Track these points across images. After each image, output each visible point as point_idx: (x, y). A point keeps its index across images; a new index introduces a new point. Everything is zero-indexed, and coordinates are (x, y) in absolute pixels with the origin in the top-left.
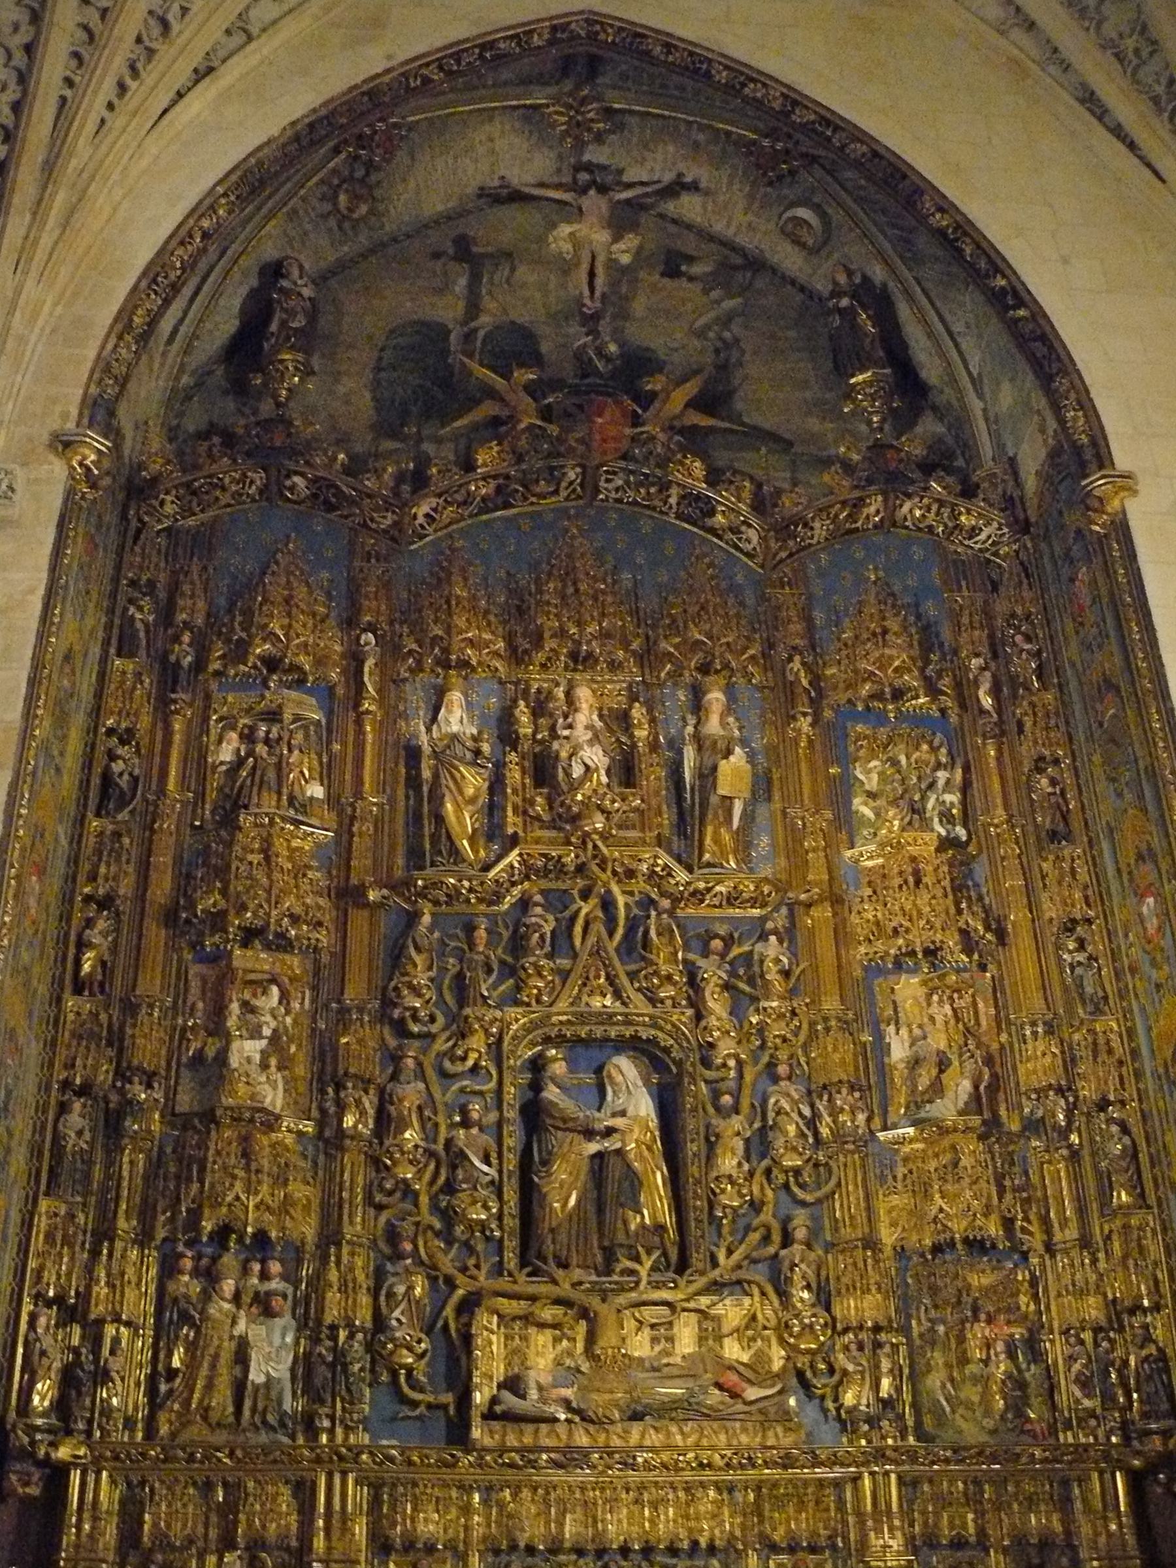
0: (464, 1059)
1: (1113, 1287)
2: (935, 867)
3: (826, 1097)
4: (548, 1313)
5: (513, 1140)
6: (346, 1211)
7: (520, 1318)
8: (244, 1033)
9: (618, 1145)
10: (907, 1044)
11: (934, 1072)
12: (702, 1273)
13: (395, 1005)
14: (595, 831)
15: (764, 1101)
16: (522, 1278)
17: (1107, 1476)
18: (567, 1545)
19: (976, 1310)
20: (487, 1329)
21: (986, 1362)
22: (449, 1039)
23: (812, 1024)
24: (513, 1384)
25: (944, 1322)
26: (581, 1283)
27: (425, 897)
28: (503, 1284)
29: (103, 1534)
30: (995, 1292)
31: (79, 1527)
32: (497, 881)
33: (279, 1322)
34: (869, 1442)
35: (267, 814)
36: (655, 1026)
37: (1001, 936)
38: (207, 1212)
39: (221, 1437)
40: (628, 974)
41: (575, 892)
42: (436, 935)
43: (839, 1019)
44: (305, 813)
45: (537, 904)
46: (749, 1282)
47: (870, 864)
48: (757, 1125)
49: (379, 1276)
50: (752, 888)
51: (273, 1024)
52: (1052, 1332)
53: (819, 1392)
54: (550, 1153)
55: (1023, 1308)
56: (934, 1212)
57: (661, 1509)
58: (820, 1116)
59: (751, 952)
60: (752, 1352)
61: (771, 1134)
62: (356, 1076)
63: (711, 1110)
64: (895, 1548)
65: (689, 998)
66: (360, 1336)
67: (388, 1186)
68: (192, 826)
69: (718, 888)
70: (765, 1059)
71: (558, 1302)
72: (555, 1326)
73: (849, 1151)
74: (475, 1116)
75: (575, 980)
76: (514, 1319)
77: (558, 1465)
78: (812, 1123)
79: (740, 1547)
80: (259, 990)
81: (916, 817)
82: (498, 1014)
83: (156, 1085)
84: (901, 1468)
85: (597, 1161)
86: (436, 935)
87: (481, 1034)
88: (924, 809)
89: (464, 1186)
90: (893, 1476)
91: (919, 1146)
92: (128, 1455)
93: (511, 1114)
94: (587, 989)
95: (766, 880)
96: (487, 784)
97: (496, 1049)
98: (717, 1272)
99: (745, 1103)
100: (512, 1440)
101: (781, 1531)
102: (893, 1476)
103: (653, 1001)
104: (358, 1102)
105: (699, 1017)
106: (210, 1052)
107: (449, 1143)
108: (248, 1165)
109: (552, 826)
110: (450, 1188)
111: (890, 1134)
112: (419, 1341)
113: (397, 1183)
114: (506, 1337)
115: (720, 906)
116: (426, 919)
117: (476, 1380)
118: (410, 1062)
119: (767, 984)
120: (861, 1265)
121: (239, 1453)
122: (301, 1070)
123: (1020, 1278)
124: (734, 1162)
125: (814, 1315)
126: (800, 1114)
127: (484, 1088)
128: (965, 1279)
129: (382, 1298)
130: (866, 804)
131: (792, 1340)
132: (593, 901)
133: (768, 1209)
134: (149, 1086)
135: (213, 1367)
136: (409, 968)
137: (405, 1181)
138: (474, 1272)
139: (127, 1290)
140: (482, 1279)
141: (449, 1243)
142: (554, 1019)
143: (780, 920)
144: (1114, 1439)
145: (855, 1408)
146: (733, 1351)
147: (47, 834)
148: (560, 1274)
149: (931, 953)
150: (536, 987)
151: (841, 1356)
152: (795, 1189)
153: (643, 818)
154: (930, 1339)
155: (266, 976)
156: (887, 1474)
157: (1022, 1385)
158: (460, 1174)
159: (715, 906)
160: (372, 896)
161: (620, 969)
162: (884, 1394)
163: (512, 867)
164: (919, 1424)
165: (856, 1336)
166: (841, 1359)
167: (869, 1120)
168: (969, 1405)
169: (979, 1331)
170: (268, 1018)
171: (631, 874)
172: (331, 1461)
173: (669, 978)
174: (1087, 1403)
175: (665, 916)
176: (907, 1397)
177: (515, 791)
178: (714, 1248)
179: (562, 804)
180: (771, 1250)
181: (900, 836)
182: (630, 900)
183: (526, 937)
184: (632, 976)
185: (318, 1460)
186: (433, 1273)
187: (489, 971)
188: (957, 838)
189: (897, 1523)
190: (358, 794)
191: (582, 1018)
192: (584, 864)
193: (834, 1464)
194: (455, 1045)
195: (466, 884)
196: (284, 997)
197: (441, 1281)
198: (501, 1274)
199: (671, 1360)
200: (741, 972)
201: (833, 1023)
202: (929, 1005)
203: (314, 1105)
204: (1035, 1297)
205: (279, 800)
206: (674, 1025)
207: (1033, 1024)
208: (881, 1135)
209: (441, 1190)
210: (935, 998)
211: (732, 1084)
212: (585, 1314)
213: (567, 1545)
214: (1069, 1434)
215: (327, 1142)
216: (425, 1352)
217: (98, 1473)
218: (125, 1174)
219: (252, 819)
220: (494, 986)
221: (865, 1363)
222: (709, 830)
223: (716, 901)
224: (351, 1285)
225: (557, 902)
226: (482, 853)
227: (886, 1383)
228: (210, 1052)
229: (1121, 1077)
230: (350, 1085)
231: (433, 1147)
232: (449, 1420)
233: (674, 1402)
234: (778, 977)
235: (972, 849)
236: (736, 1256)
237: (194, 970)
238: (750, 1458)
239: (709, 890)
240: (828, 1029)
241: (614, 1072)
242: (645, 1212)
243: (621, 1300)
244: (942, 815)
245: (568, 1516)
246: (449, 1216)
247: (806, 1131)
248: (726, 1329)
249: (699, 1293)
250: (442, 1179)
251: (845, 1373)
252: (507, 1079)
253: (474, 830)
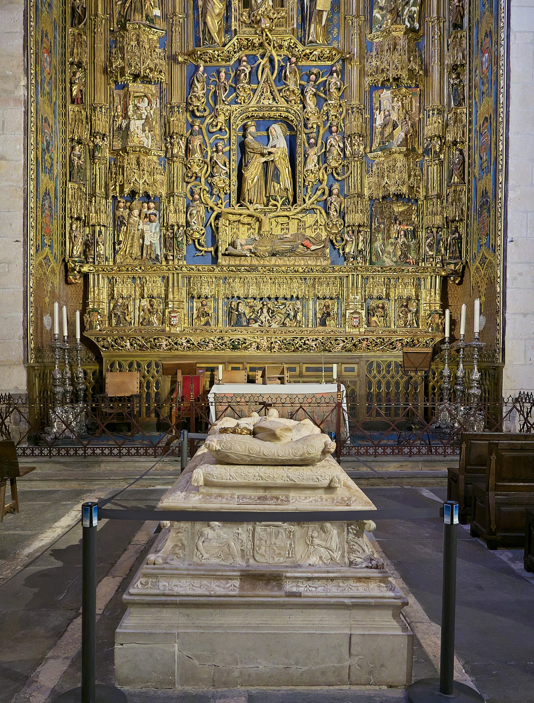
0: (217, 126)
1: (447, 212)
2: (402, 42)
3: (349, 140)
4: (246, 220)
5: (235, 157)
6: (175, 184)
7: (236, 221)
8: (135, 117)
9: (272, 159)
10: (382, 118)
11: (391, 129)
12: (300, 205)
13: (190, 104)
14: (266, 28)
15: (327, 141)
16: (237, 207)
17: (433, 278)
18: (250, 296)
19: (396, 219)
20: (224, 225)
21: (396, 239)
22: (211, 118)
23: (347, 110)
24: (233, 244)
25: (383, 223)
26: (257, 209)
27: (201, 59)
28: (230, 210)
29: (102, 294)
31: (94, 292)
32: (228, 51)
33: (154, 224)
34: (353, 264)
35: (137, 23)
36: (287, 111)
37: (426, 72)
38: (126, 186)
39: (137, 262)
40: (278, 90)
41: (258, 55)
42: (205, 75)
43: (358, 108)
44: (153, 23)
45: (244, 61)
46: (316, 209)
47: (377, 40)
48: (323, 150)
49: (188, 207)
50: (328, 52)
51: (146, 114)
52: (422, 228)
53: (337, 247)
54: (248, 162)
55: (413, 220)
56: (384, 183)
57: (282, 286)
58: (347, 147)
59: (326, 80)
60: (316, 233)
61: (328, 154)
62: (177, 133)
63: (307, 145)
64: (358, 299)
65: (301, 99)
66: (181, 228)
67: (189, 175)
68: (110, 30)
69: (315, 53)
70: (329, 125)
71: (249, 216)
72: (248, 224)
73: (356, 161)
74: (220, 148)
75: (258, 93)
76: (234, 222)
77: (249, 271)
78: (343, 150)
79: (307, 297)
80: (141, 100)
81: (399, 18)
82: (229, 107)
83: (105, 139)
84: (363, 273)
85: (265, 164)
86: (205, 75)
87: (222, 116)
88: (403, 14)
89: (216, 174)
90: (360, 276)
91: (383, 159)
92: (107, 269)
93: (234, 147)
94: (263, 97)
95: (334, 48)
96: (225, 6)
97: (228, 122)
98: (305, 205)
99: (320, 142)
100: (232, 263)
101: (321, 293)
102: (360, 276)
103: (287, 101)
104: (178, 143)
105: (304, 107)
106: (124, 125)
107: (211, 158)
108: (139, 168)
109: (250, 25)
110: (212, 176)
111: (372, 155)
112: (202, 230)
113: (193, 174)
114: (231, 229)
115: (316, 61)
116: (202, 69)
117: (220, 243)
118: (196, 128)
119: (330, 94)
120: (356, 203)
121: (143, 268)
122: (157, 132)
123: (413, 209)
124: (313, 165)
125: (337, 221)
126: (339, 146)
127: (224, 137)
129: (188, 215)
130: (379, 13)
131: (329, 229)
132: (266, 59)
133: (325, 183)
134: (103, 139)
135: (132, 240)
136: (196, 89)
137: (195, 173)
138: (220, 205)
139: (101, 214)
140: (223, 207)
141: (212, 194)
142: (250, 109)
143: (338, 67)
144: (438, 265)
145: (349, 253)
146: (309, 233)
147: (49, 35)
148: (250, 206)
149: (396, 79)
150: (243, 96)
151: (346, 235)
152: (335, 175)
153: (287, 20)
154: (378, 230)
155: (143, 94)
156: (358, 275)
157: (408, 247)
158: (215, 169)
159: (313, 61)
160: (180, 59)
161: (276, 89)
162: (359, 248)
163: (234, 45)
164: (371, 258)
165: (352, 228)
166: (346, 237)
167: (365, 148)
168: (389, 253)
169: (397, 227)
170: (144, 111)
171: (281, 47)
172: (173, 270)
173: (293, 91)
174: (431, 253)
175: (293, 65)
176: (368, 250)
177: (236, 11)
178: (304, 197)
179: (254, 15)
180: (325, 197)
181: (390, 27)
182: (280, 58)
183: (239, 76)
184: (280, 91)
185: (169, 270)
186: (207, 206)
187: (226, 90)
188: (414, 28)
189: (359, 291)
190: (174, 14)
191: (260, 109)
192: (262, 43)
193: (340, 271)
194: (213, 120)
195: (216, 52)
196: (150, 102)
197: (209, 208)
198: (230, 206)
199: (287, 236)
200: (322, 89)
201: (354, 110)
202: (393, 102)
203: (163, 145)
204: (418, 216)
205: (142, 17)
206: (294, 111)
207: (433, 110)
208: (369, 155)
209: (209, 176)
210: (396, 99)
211: (314, 135)
212: (258, 219)
213: (250, 296)
214: (423, 263)
215: (168, 159)
216: (203, 234)
217: (98, 275)
218: (98, 173)
219: (131, 26)
220: (228, 96)
221: (353, 238)
222: (313, 26)
223: (314, 58)
224: (177, 211)
225: (252, 59)
226: (223, 39)
227: (360, 244)
228: (124, 125)
229: (463, 132)
230: (175, 137)
231: (206, 160)
232: (212, 256)
233: (287, 250)
234: (335, 91)
235: (421, 32)
236: (311, 200)
237: (116, 92)
238: (312, 269)
239: (311, 53)
240: (353, 112)
241: (273, 130)
242: (281, 183)
243: (272, 215)
244: (409, 17)
245: (251, 287)
246: (211, 185)
247: (340, 153)
248: (307, 226)
249: (298, 213)
250: (208, 173)
251: (347, 240)
252: (232, 134)
253: (219, 29)
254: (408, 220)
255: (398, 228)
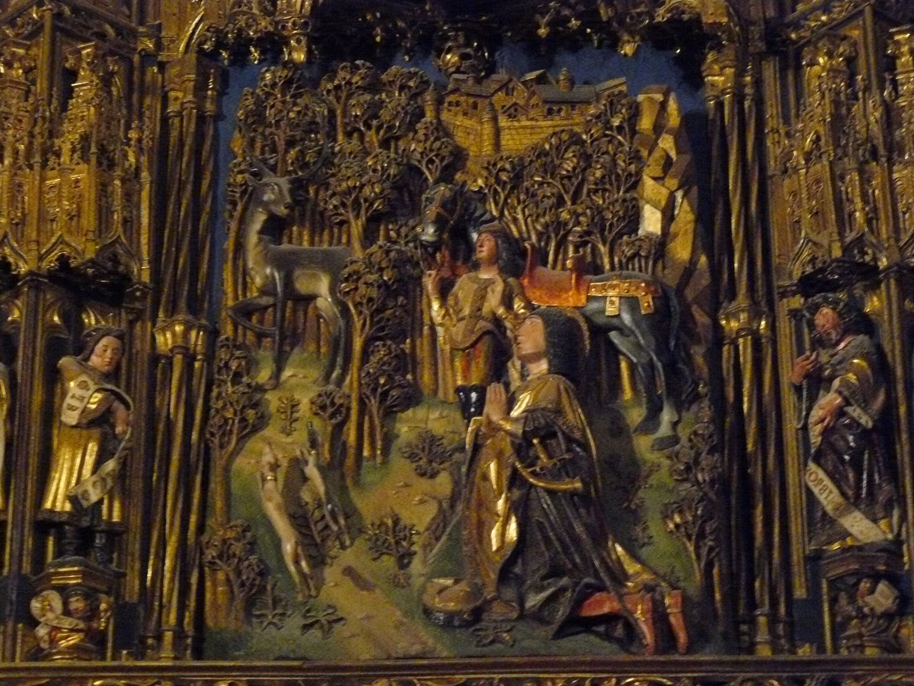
30: (550, 170)
123: (646, 123)
128: (441, 130)
254: (599, 225)
255: (493, 302)
